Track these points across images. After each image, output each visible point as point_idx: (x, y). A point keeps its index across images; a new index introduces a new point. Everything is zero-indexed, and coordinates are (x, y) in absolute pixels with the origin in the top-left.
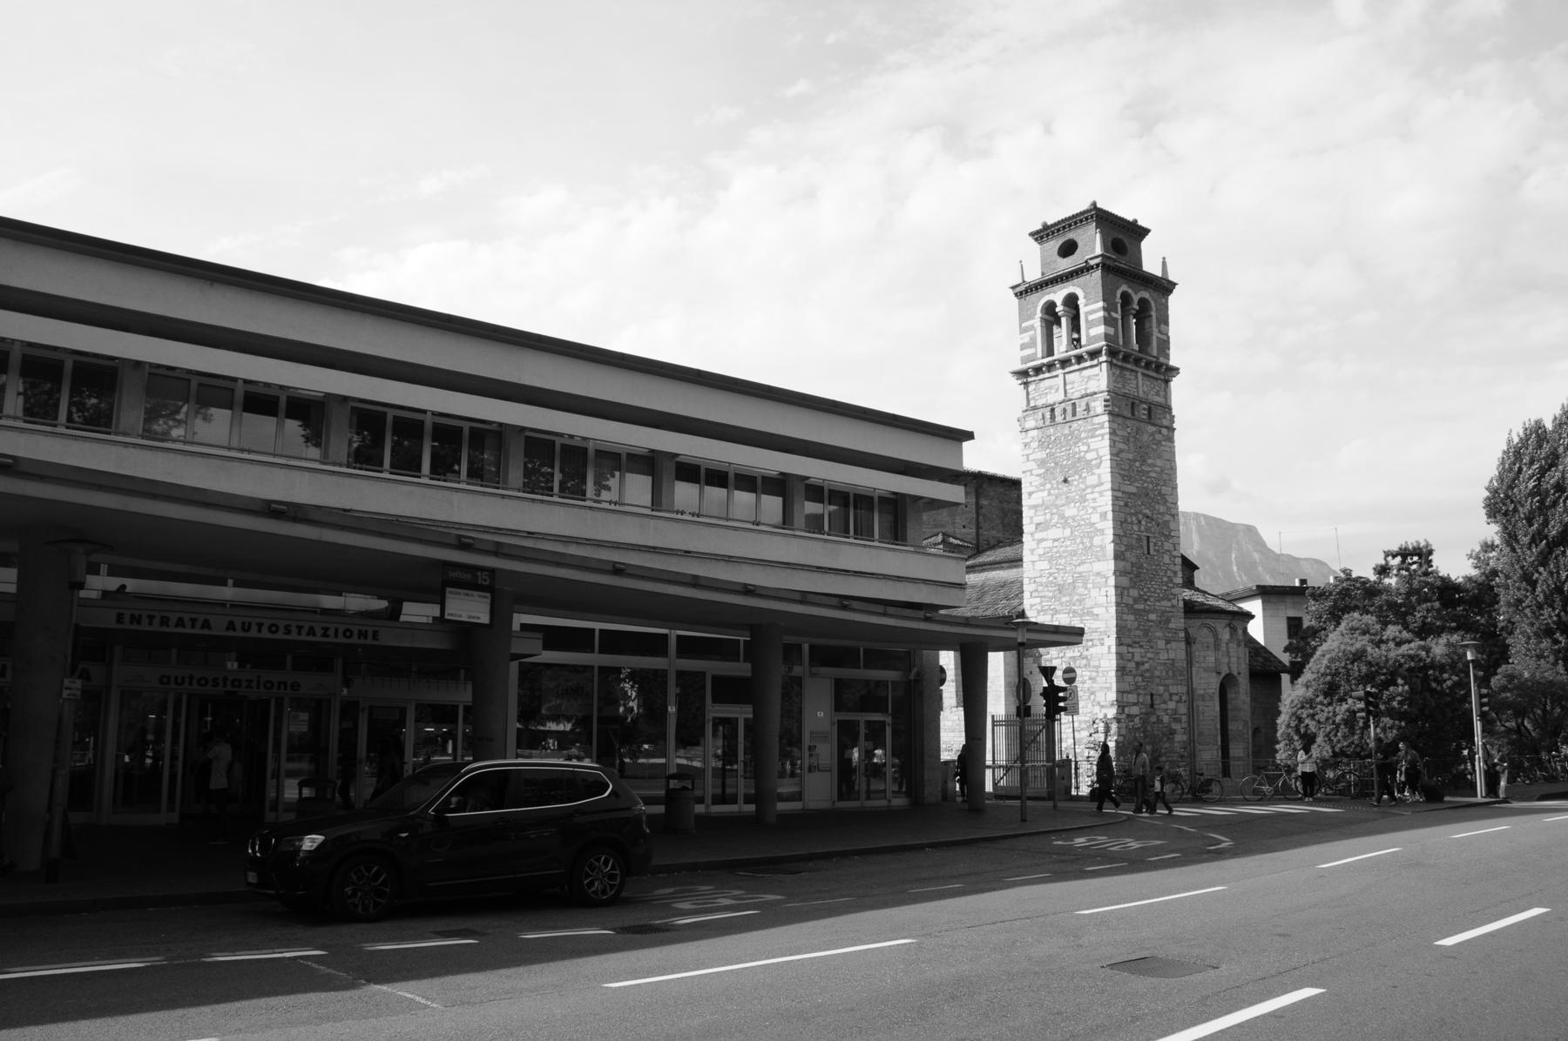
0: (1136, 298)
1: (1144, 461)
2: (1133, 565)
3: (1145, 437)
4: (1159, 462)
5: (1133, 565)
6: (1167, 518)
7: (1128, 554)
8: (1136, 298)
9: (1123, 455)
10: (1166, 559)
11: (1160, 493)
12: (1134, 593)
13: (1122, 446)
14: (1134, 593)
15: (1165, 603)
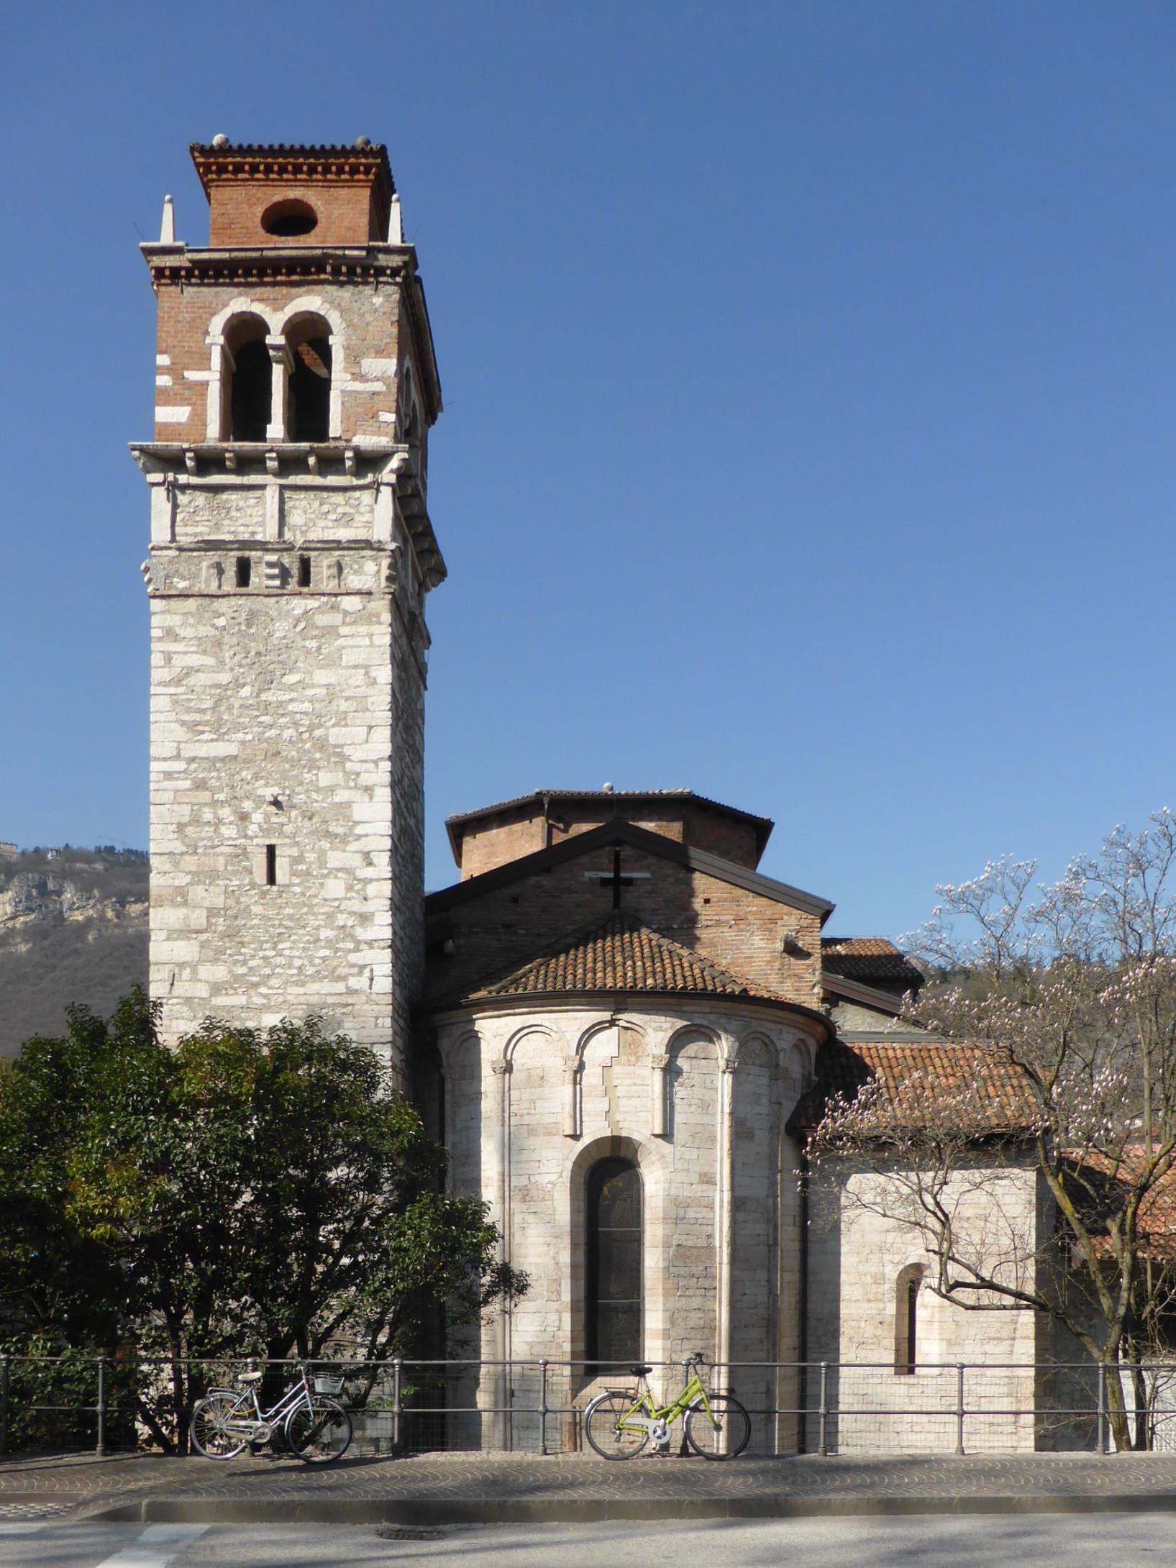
0: (276, 321)
1: (268, 682)
2: (212, 912)
3: (281, 628)
4: (322, 676)
5: (212, 912)
6: (341, 796)
7: (198, 892)
8: (276, 321)
9: (201, 679)
10: (335, 888)
11: (322, 745)
12: (219, 972)
13: (195, 660)
14: (219, 972)
15: (326, 987)
